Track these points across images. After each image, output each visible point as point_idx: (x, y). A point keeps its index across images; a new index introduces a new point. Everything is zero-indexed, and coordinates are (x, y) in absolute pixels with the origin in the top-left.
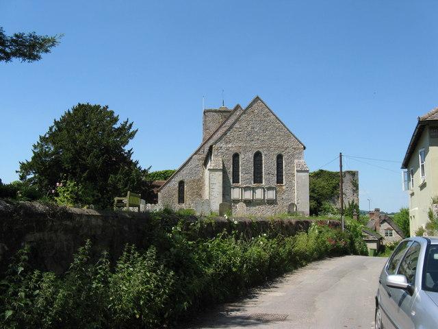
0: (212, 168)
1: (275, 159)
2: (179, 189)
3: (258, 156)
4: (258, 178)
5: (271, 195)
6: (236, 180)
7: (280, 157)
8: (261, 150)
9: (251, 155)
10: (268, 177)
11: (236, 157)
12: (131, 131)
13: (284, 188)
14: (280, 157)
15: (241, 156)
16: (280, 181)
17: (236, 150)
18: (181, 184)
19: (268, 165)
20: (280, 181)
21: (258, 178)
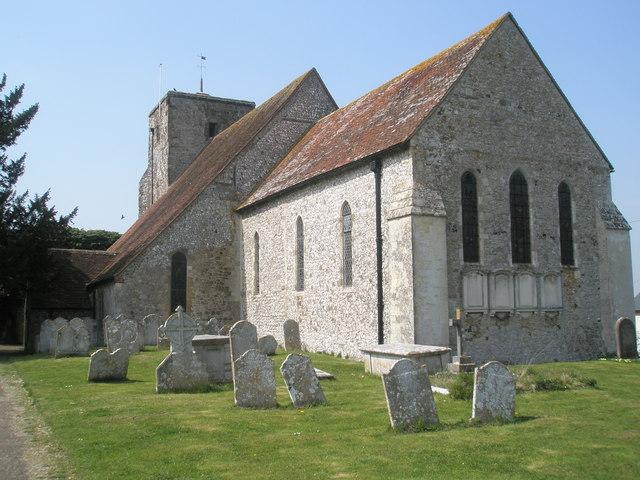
0: (419, 211)
1: (555, 195)
2: (173, 275)
3: (518, 183)
4: (521, 253)
5: (552, 295)
6: (471, 254)
7: (564, 192)
8: (525, 169)
9: (504, 181)
10: (544, 248)
11: (469, 182)
12: (17, 111)
13: (577, 274)
14: (564, 192)
15: (484, 182)
16: (567, 258)
17: (463, 162)
18: (179, 261)
19: (542, 216)
20: (567, 258)
21: (521, 253)
